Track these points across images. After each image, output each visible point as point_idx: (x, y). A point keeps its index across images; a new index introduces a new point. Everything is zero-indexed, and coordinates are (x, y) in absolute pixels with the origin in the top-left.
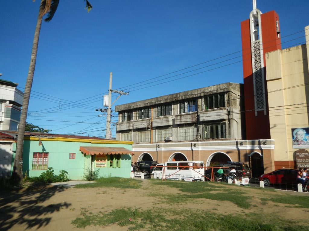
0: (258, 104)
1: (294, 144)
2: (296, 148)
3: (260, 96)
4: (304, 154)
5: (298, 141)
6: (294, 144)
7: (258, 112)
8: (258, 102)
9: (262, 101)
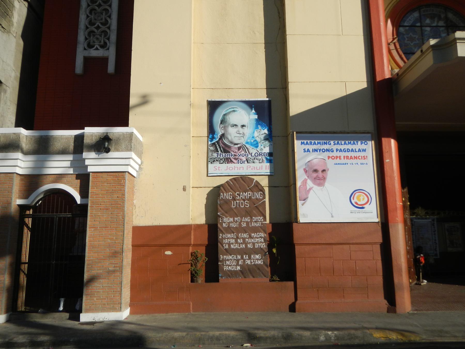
0: (91, 33)
1: (210, 160)
2: (218, 172)
3: (99, 10)
4: (247, 195)
5: (226, 150)
6: (210, 160)
7: (87, 60)
8: (93, 28)
9: (103, 28)
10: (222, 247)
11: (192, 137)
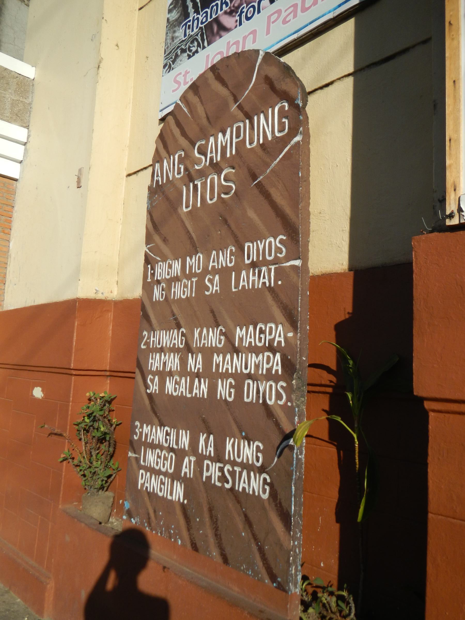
10: (142, 388)
11: (140, 9)
